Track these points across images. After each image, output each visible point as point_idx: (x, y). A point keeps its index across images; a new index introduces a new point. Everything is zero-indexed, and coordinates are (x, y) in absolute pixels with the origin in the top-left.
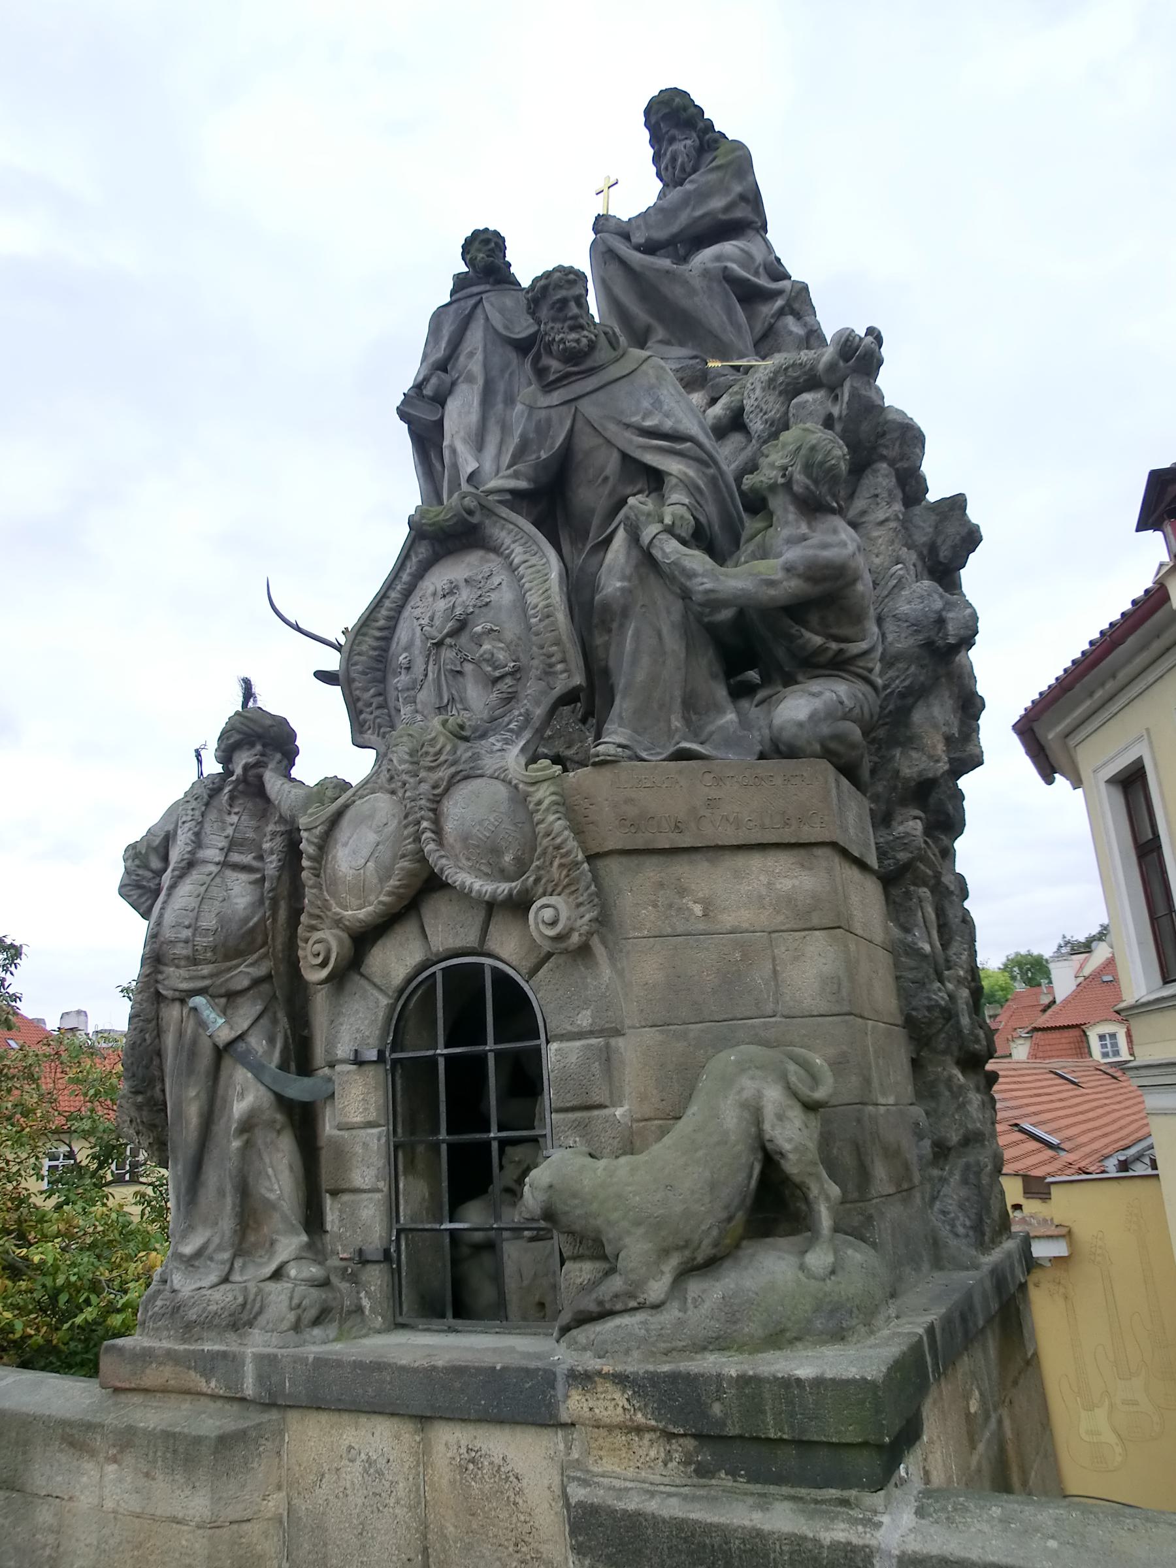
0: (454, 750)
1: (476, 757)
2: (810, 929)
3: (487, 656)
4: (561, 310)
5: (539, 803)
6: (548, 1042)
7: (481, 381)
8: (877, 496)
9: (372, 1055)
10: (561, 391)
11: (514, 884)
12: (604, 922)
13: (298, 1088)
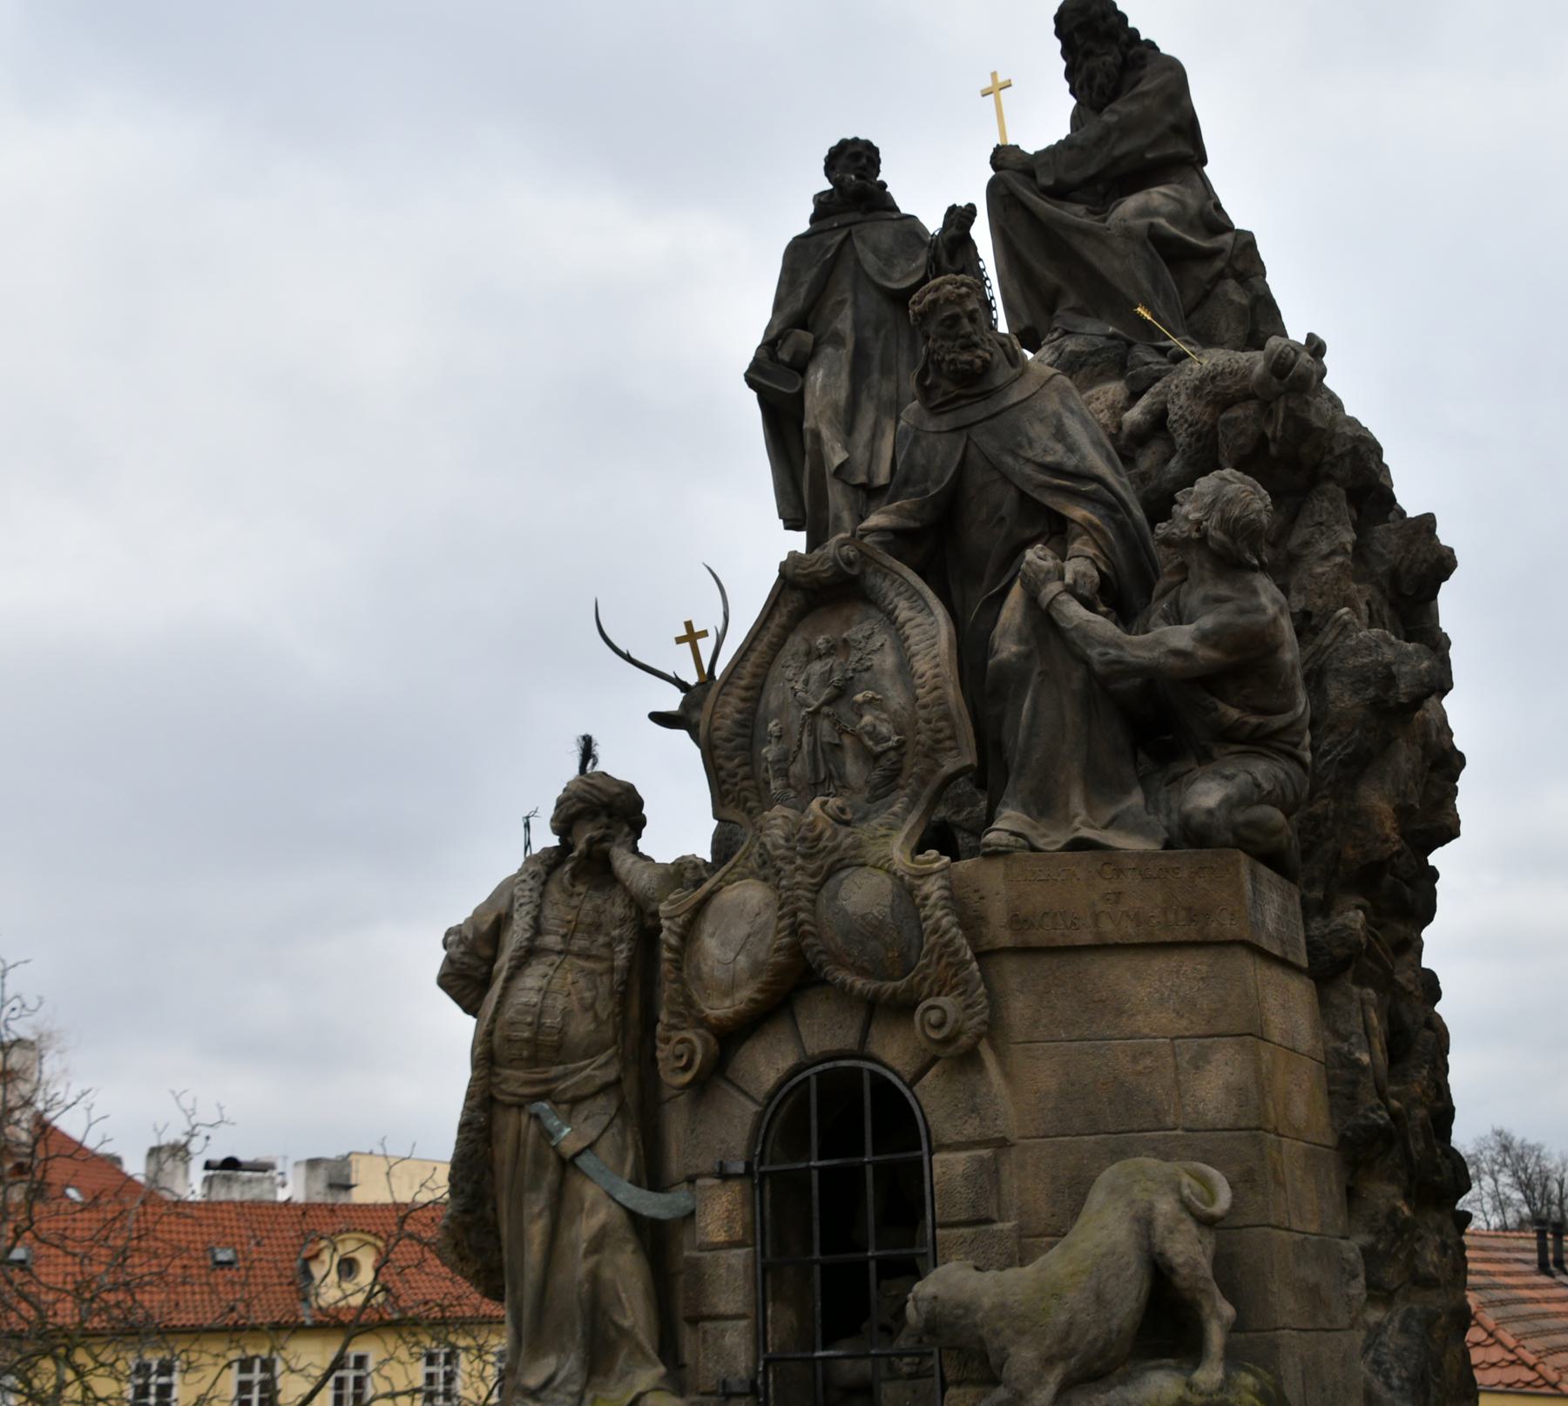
0: (835, 834)
1: (858, 845)
2: (1218, 1036)
3: (869, 728)
4: (950, 327)
6: (931, 1153)
7: (850, 345)
8: (1321, 524)
9: (740, 1167)
11: (898, 983)
12: (994, 1029)
13: (652, 1205)
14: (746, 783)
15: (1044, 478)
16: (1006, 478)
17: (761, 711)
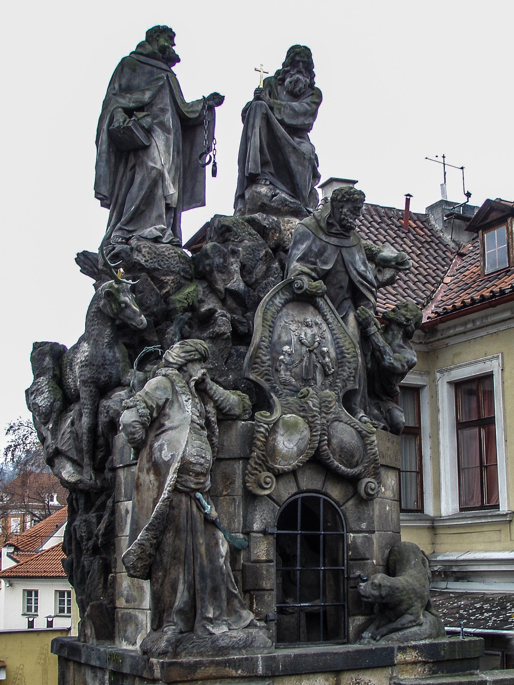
5: (373, 441)
10: (336, 239)
14: (268, 368)
15: (360, 278)
16: (347, 272)
17: (276, 338)
